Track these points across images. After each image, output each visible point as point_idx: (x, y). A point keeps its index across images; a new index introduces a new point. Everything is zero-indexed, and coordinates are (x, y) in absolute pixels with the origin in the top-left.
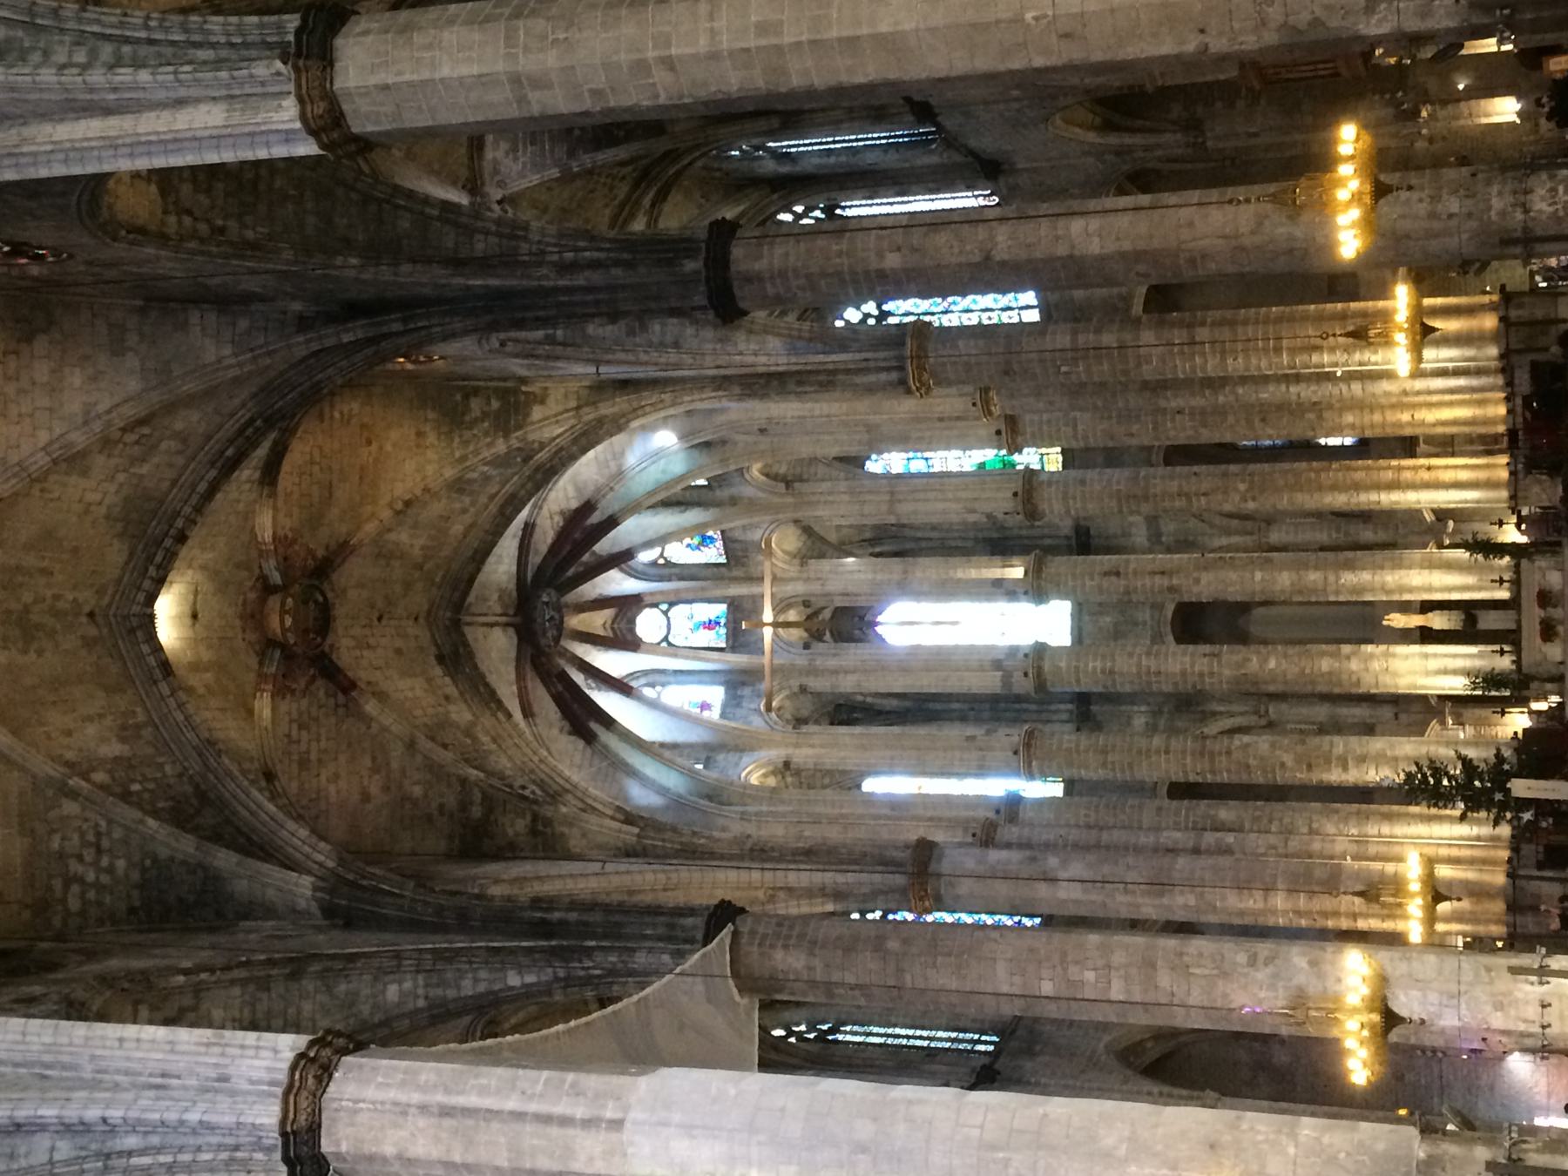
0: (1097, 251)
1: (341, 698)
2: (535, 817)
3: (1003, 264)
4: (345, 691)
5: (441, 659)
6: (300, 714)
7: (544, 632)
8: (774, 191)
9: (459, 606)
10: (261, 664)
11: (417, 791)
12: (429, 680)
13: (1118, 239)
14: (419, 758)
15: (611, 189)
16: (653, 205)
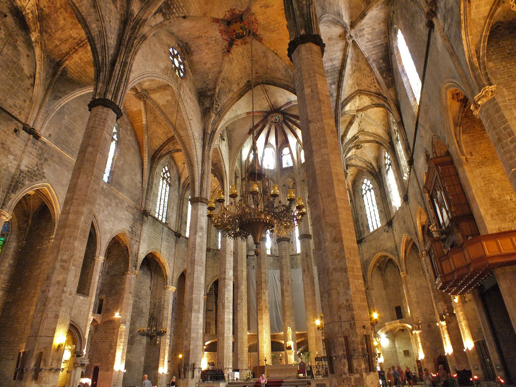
0: (315, 161)
1: (226, 50)
2: (210, 108)
3: (309, 128)
4: (227, 50)
5: (249, 82)
6: (218, 39)
7: (272, 117)
8: (389, 143)
9: (263, 83)
10: (222, 19)
11: (210, 77)
12: (241, 78)
13: (321, 168)
14: (217, 75)
15: (372, 84)
16: (374, 104)
